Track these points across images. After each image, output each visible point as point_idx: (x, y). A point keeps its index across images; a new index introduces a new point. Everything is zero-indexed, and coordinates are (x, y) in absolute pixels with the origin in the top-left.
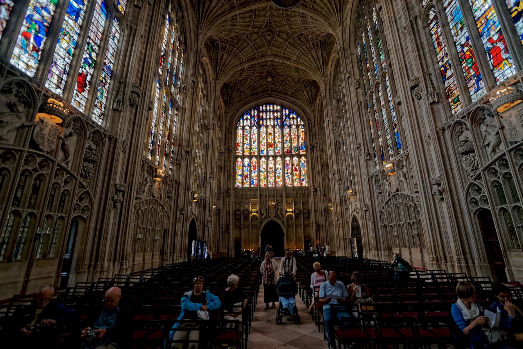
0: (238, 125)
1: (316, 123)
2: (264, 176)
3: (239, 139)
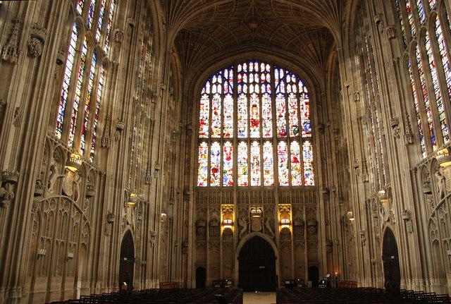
0: (203, 92)
1: (328, 91)
3: (204, 113)
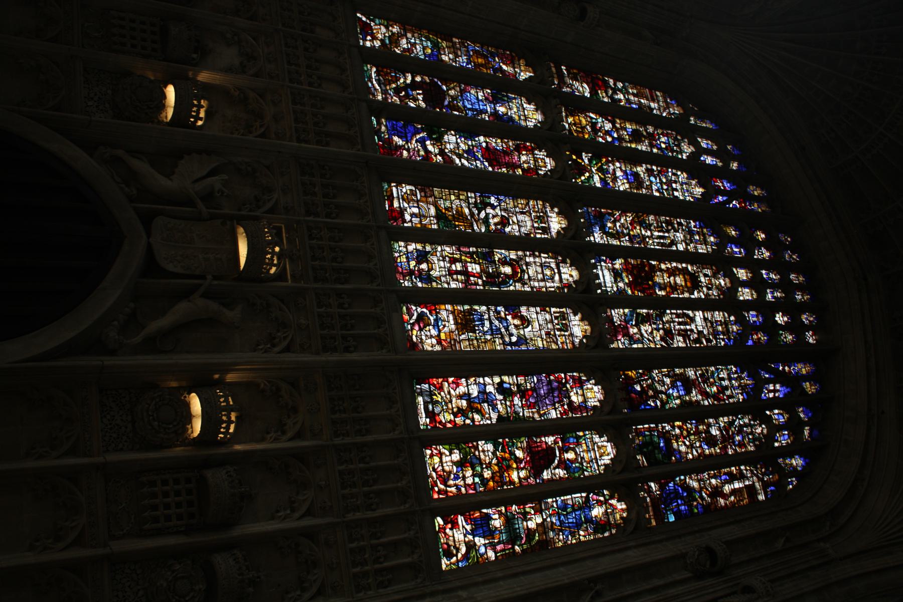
2: (460, 215)
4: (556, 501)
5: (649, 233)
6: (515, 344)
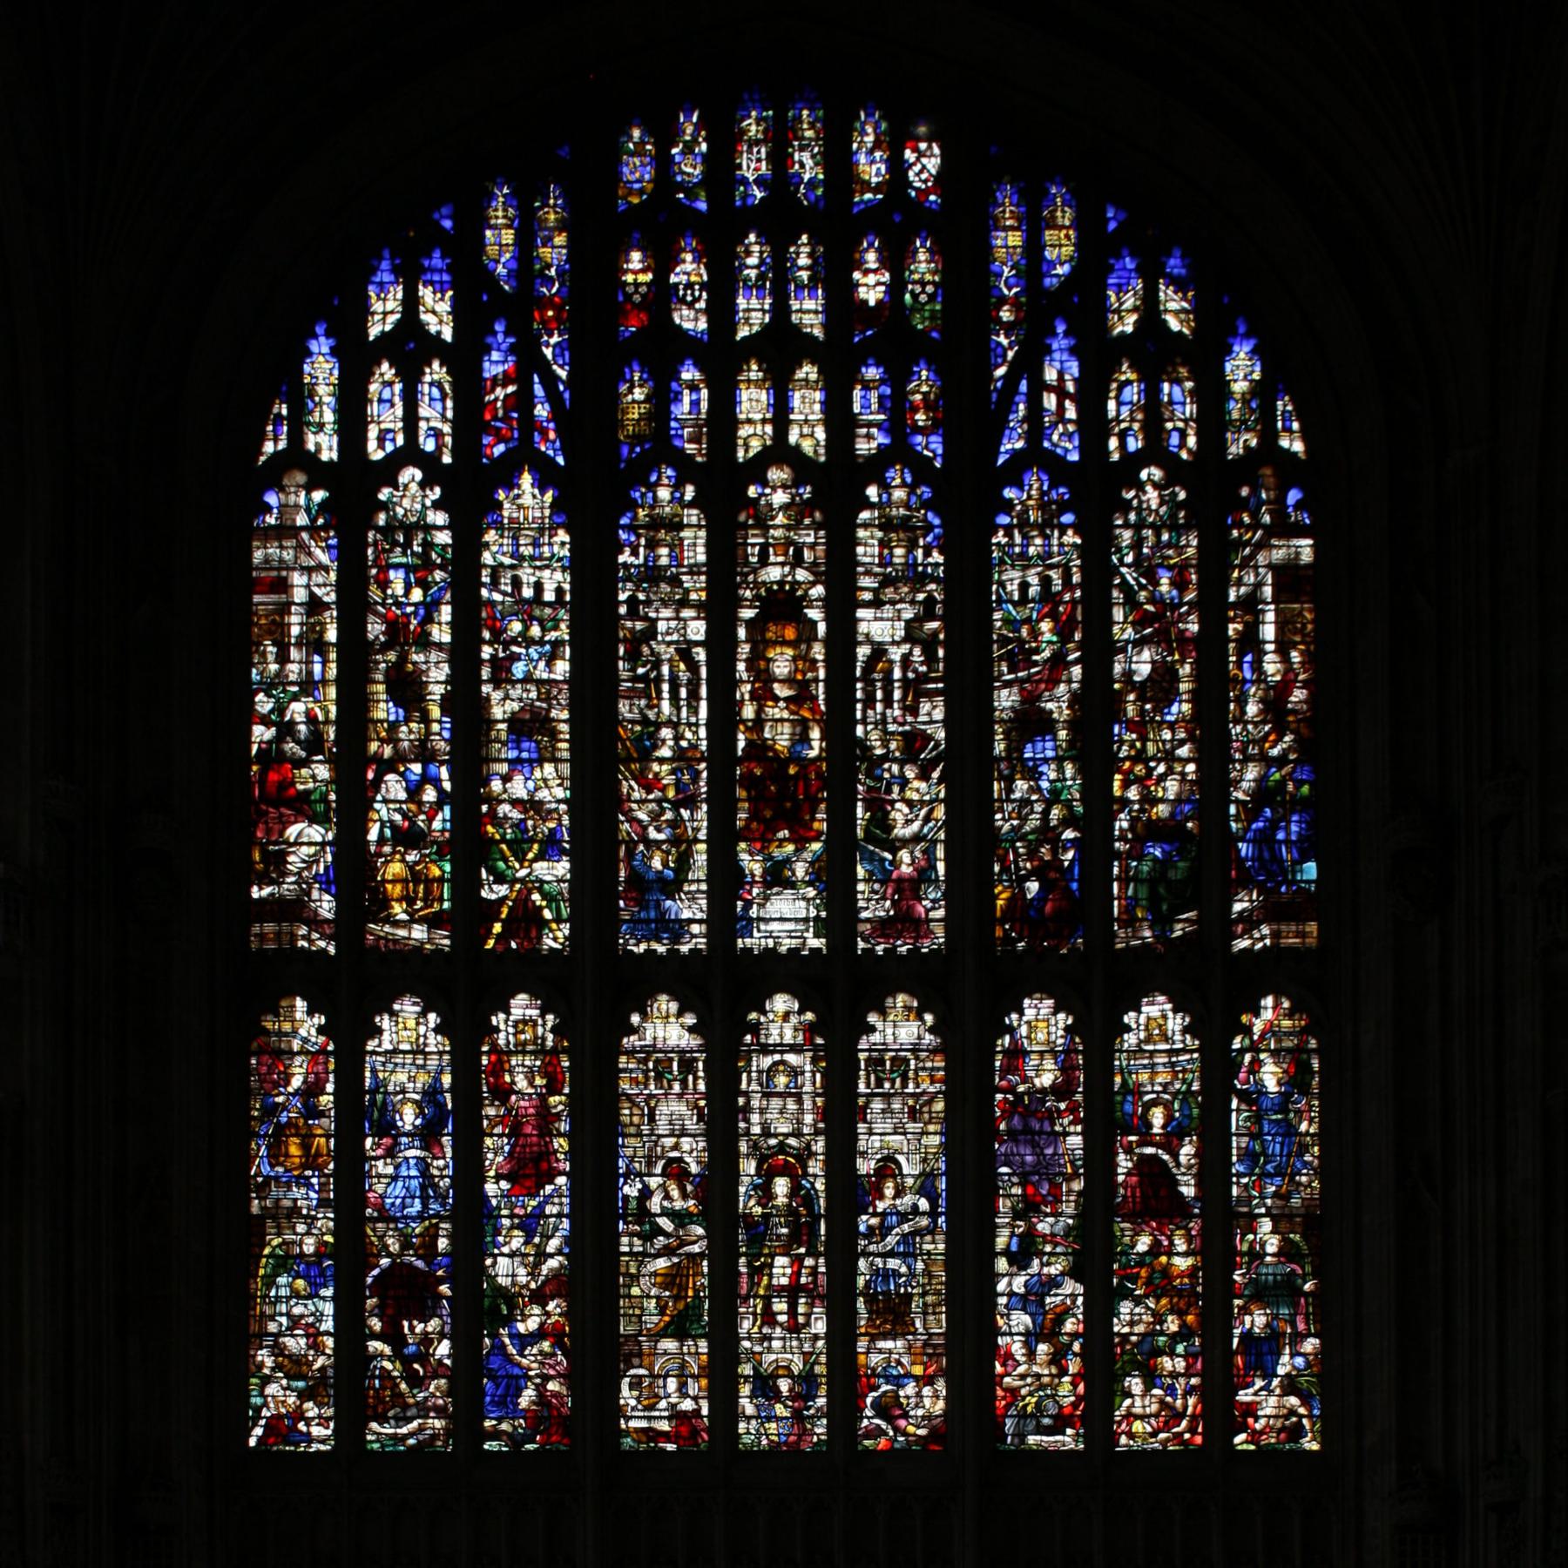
2: (672, 1280)
4: (1239, 1175)
5: (666, 733)
6: (934, 1203)
